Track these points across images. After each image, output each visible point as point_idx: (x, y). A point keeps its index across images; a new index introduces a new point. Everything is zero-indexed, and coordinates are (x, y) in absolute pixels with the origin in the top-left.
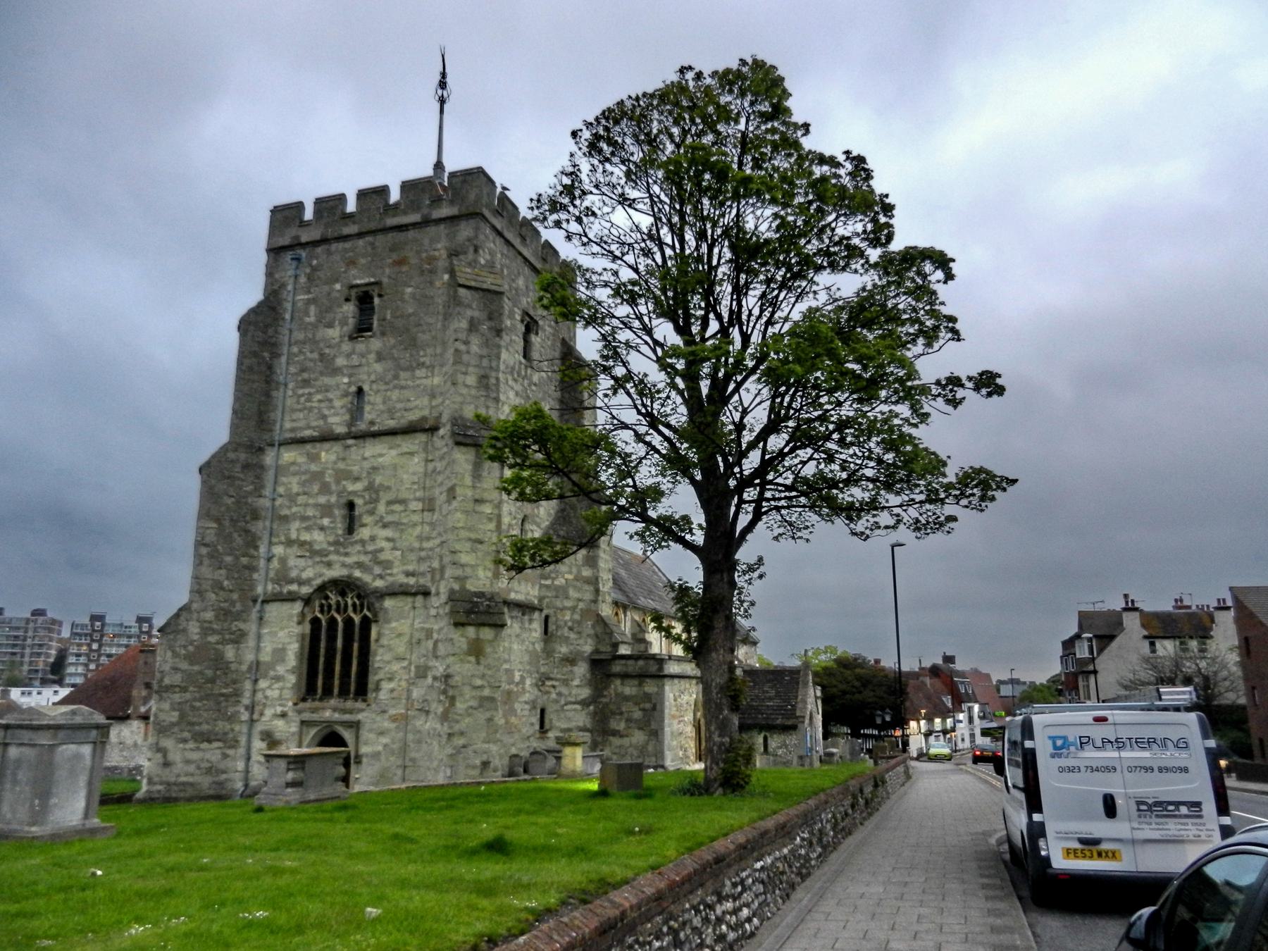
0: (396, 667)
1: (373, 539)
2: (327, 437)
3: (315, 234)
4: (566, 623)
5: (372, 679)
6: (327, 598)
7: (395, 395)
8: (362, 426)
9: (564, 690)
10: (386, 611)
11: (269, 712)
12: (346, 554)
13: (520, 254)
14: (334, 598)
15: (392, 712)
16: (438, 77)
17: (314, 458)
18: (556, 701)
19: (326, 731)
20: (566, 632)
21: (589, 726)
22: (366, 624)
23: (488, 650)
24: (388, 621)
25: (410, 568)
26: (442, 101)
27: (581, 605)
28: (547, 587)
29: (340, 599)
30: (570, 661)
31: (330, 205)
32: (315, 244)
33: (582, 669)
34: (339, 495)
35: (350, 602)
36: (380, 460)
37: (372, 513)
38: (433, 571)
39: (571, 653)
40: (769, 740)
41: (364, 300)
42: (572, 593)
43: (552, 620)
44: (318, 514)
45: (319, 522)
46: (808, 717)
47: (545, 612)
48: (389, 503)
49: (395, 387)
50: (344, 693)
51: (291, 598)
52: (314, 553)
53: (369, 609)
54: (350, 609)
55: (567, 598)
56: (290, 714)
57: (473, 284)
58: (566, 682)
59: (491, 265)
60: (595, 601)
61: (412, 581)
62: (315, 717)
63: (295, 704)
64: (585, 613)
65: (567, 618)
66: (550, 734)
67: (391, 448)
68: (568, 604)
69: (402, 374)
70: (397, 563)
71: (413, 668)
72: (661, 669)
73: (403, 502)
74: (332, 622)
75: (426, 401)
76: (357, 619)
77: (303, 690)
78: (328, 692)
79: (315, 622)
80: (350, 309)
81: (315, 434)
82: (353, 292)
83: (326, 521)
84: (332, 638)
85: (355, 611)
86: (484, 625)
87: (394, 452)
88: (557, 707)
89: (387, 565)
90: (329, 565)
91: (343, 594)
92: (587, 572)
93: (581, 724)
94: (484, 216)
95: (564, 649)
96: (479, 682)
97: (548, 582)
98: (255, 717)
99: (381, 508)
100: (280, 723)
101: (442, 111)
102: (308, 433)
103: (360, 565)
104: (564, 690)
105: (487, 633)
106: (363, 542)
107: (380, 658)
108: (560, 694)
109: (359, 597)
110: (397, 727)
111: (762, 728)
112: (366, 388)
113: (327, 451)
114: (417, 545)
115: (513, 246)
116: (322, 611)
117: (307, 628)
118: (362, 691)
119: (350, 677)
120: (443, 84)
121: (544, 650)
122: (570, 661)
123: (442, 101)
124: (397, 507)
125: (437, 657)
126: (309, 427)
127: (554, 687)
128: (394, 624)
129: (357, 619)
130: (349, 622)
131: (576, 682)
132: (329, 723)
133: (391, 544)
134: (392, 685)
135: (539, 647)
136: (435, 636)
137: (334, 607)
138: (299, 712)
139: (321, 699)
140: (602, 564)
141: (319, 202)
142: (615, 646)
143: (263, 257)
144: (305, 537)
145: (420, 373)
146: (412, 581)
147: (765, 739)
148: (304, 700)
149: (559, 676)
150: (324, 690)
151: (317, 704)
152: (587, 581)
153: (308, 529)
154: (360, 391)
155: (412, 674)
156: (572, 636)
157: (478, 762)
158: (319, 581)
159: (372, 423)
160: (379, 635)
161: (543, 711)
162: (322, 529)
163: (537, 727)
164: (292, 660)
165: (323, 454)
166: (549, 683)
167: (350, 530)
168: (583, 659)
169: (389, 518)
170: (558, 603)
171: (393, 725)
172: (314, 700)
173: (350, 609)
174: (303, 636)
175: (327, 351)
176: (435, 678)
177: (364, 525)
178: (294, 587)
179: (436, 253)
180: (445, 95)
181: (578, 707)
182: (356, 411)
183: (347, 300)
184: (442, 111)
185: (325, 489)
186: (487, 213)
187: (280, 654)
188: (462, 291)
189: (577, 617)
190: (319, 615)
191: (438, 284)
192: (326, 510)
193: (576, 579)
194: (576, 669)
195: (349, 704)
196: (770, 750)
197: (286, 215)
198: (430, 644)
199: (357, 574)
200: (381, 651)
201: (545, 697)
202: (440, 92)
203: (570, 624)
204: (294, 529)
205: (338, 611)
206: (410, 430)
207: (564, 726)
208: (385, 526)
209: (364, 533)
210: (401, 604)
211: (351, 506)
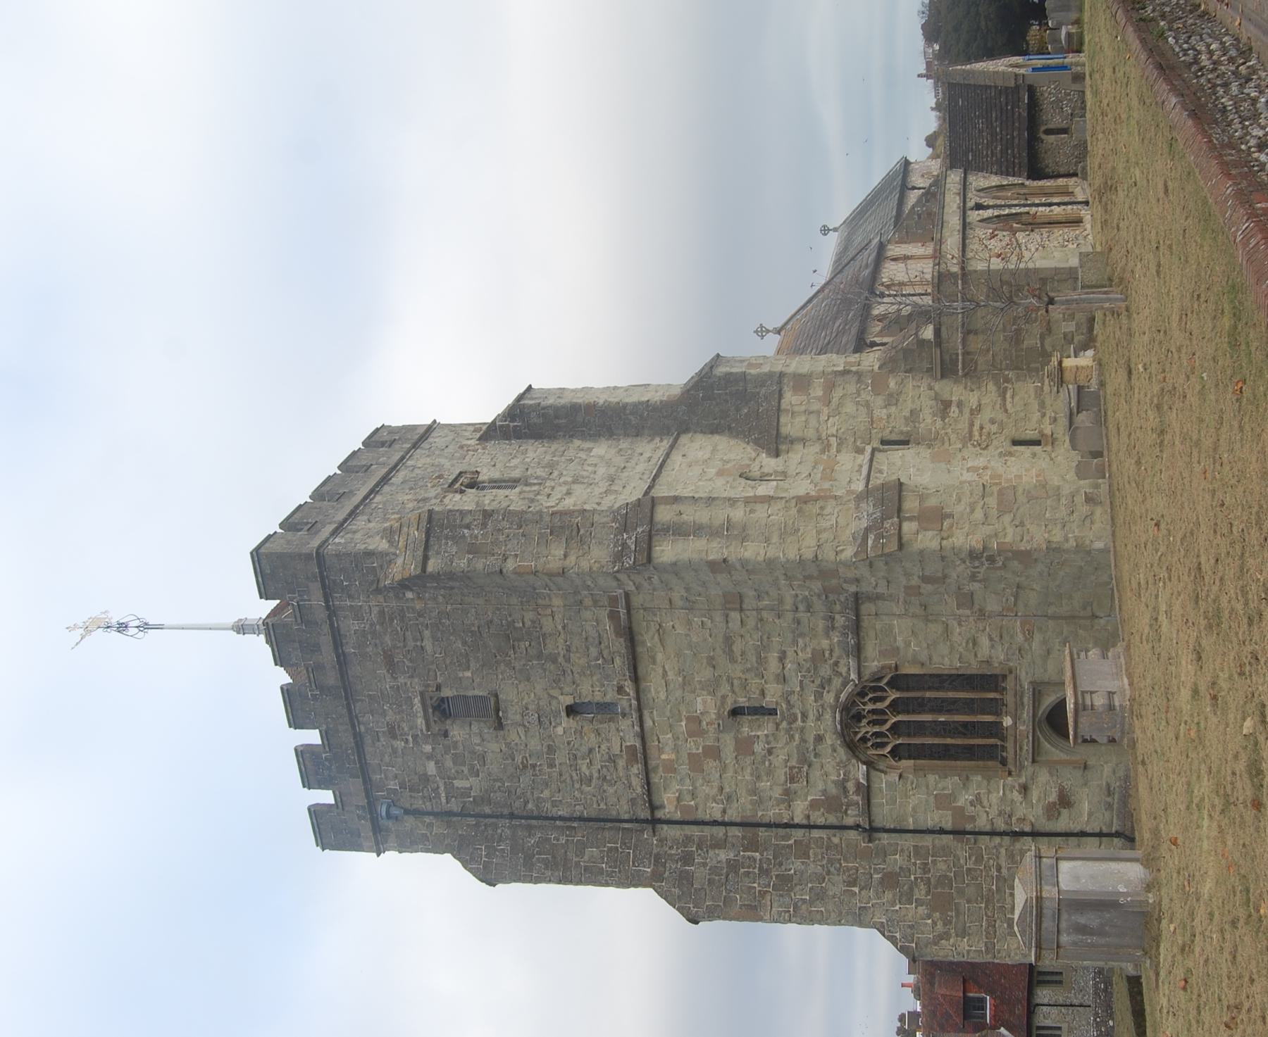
0: (959, 634)
1: (783, 679)
2: (642, 754)
3: (355, 785)
5: (974, 668)
6: (864, 739)
7: (579, 660)
11: (1021, 810)
12: (805, 716)
13: (365, 498)
14: (865, 729)
15: (1020, 638)
16: (114, 634)
17: (670, 768)
19: (1046, 728)
22: (898, 681)
23: (932, 502)
25: (821, 624)
26: (145, 627)
29: (864, 721)
31: (312, 768)
32: (367, 781)
33: (953, 390)
35: (870, 707)
36: (671, 675)
38: (826, 591)
40: (1051, 126)
41: (442, 709)
44: (749, 760)
45: (759, 759)
46: (1016, 70)
48: (733, 660)
49: (568, 660)
50: (996, 707)
51: (867, 792)
52: (803, 760)
53: (880, 679)
54: (879, 706)
56: (1023, 780)
57: (420, 553)
59: (389, 534)
60: (859, 375)
61: (840, 620)
62: (1027, 747)
63: (1010, 774)
66: (1048, 431)
67: (654, 663)
69: (550, 648)
71: (961, 612)
72: (954, 275)
73: (728, 641)
74: (895, 729)
75: (587, 614)
76: (893, 695)
77: (990, 763)
78: (995, 730)
79: (896, 753)
80: (457, 732)
81: (636, 769)
82: (436, 728)
83: (758, 748)
84: (920, 728)
85: (882, 699)
86: (899, 510)
87: (660, 657)
90: (819, 739)
91: (858, 717)
94: (320, 547)
96: (978, 515)
98: (1027, 829)
99: (737, 671)
100: (1035, 794)
101: (159, 627)
102: (637, 783)
103: (818, 696)
104: (987, 414)
105: (911, 505)
106: (787, 696)
107: (946, 661)
109: (862, 694)
110: (1040, 629)
111: (1033, 140)
112: (569, 700)
113: (661, 751)
114: (789, 616)
115: (357, 507)
116: (883, 745)
117: (906, 763)
118: (991, 681)
119: (972, 699)
120: (122, 627)
123: (145, 627)
124: (737, 648)
125: (945, 577)
126: (628, 777)
127: (982, 428)
128: (900, 642)
129: (893, 695)
130: (895, 706)
132: (1036, 724)
133: (790, 654)
134: (984, 642)
136: (915, 581)
137: (877, 729)
138: (1022, 767)
139: (1003, 739)
140: (805, 369)
141: (308, 783)
142: (922, 343)
143: (391, 856)
144: (781, 774)
145: (548, 625)
146: (840, 620)
147: (1049, 132)
148: (1004, 762)
150: (991, 736)
151: (1010, 745)
152: (830, 387)
153: (770, 772)
154: (571, 711)
155: (968, 612)
157: (1085, 509)
158: (842, 753)
159: (620, 690)
160: (915, 661)
161: (1016, 443)
162: (770, 752)
163: (1037, 449)
164: (951, 782)
165: (663, 757)
167: (772, 712)
171: (1038, 637)
172: (1004, 748)
173: (879, 706)
174: (916, 770)
175: (519, 759)
176: (973, 577)
178: (851, 786)
179: (375, 611)
180: (137, 623)
182: (605, 709)
183: (446, 735)
184: (159, 627)
185: (714, 752)
186: (315, 543)
187: (943, 801)
188: (432, 566)
190: (889, 748)
191: (419, 606)
192: (744, 747)
195: (1009, 699)
196: (1064, 125)
197: (331, 831)
198: (928, 588)
199: (829, 698)
200: (935, 659)
202: (132, 631)
204: (772, 788)
205: (886, 721)
206: (630, 636)
209: (773, 695)
210: (872, 634)
211: (736, 712)
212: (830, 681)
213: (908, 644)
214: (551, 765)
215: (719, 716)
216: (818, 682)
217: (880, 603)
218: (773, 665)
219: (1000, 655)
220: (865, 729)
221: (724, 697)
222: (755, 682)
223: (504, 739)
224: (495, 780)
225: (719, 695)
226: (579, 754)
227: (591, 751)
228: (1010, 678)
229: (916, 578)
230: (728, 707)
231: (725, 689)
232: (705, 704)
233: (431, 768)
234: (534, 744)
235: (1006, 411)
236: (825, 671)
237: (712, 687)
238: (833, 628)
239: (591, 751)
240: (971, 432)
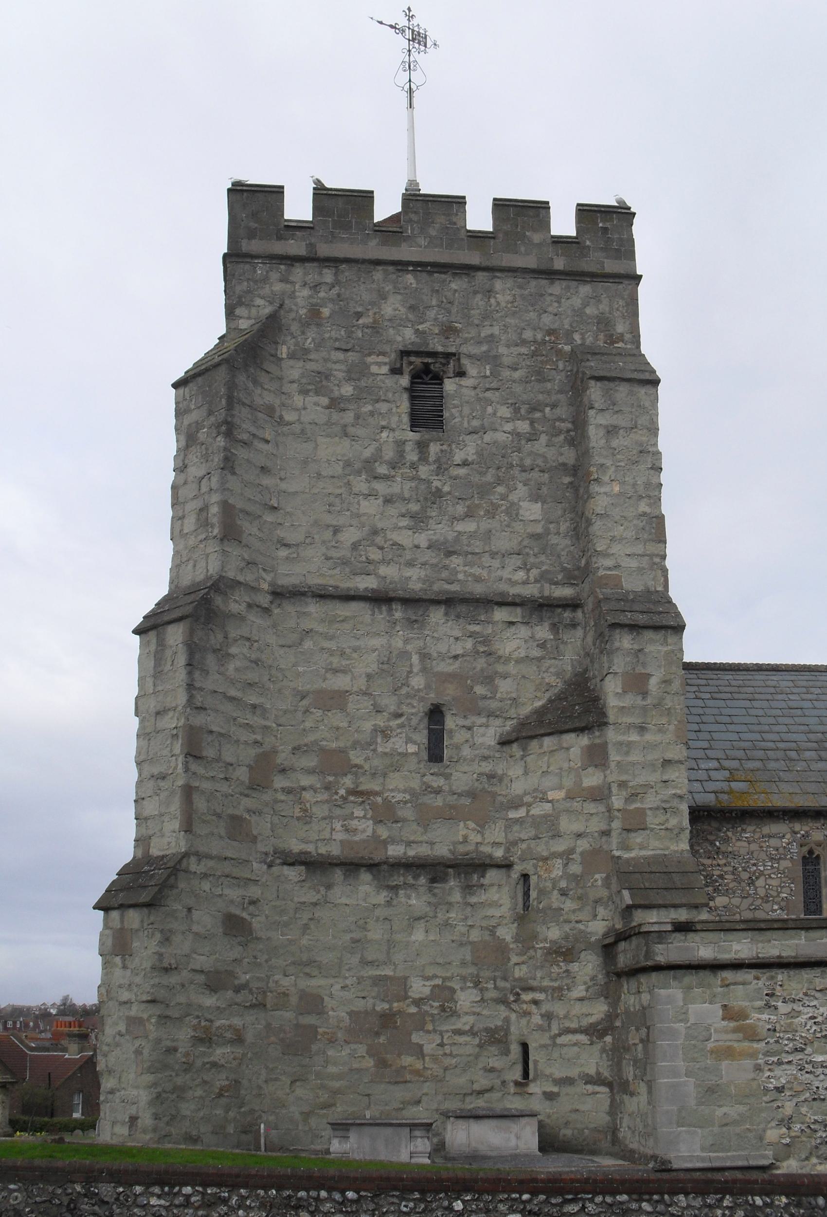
4: (555, 882)
9: (559, 1009)
18: (540, 1028)
20: (555, 899)
21: (606, 1074)
27: (583, 845)
28: (518, 821)
30: (565, 953)
33: (588, 966)
39: (566, 937)
42: (567, 825)
43: (533, 880)
47: (518, 869)
55: (557, 835)
58: (558, 993)
64: (592, 858)
65: (557, 872)
68: (560, 846)
88: (545, 1039)
92: (592, 779)
93: (592, 1071)
95: (554, 933)
97: (521, 813)
108: (548, 1017)
121: (517, 939)
122: (565, 953)
127: (536, 1002)
131: (579, 991)
135: (507, 933)
149: (546, 983)
156: (569, 905)
166: (527, 997)
168: (589, 946)
170: (541, 849)
181: (583, 1038)
189: (575, 868)
193: (570, 797)
194: (574, 967)
201: (524, 1021)
203: (563, 884)
207: (558, 1075)
235: (560, 1035)
240: (532, 989)
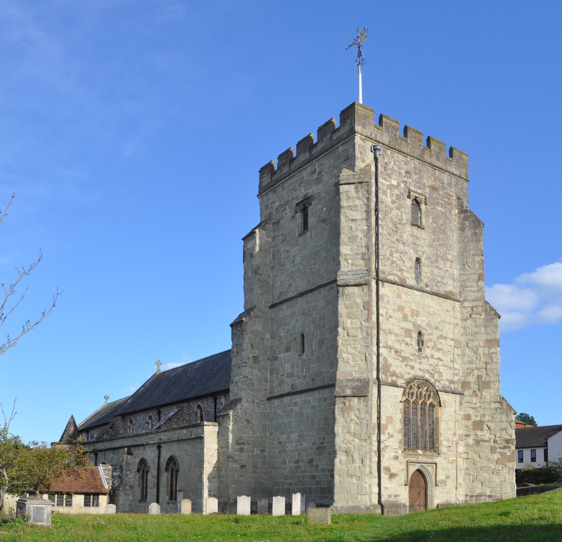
8: (422, 285)
10: (444, 401)
24: (445, 407)
34: (414, 324)
36: (432, 309)
37: (430, 340)
61: (452, 386)
70: (444, 374)
89: (440, 374)
106: (426, 357)
128: (447, 409)
146: (452, 386)
169: (439, 346)
175: (400, 226)
177: (428, 347)
198: (470, 423)
208: (439, 350)
209: (427, 352)
211: (420, 333)
212: (433, 377)
213: (446, 413)
214: (397, 240)
215: (419, 326)
216: (432, 372)
217: (459, 403)
218: (437, 355)
219: (443, 449)
220: (424, 391)
221: (426, 330)
222: (430, 344)
223: (408, 223)
224: (390, 211)
225: (427, 328)
226: (402, 256)
227: (404, 261)
228: (436, 454)
229: (479, 419)
230: (423, 331)
231: (429, 331)
232: (422, 321)
233: (394, 183)
234: (405, 236)
236: (436, 376)
237: (429, 325)
238: (450, 383)
239: (404, 261)
